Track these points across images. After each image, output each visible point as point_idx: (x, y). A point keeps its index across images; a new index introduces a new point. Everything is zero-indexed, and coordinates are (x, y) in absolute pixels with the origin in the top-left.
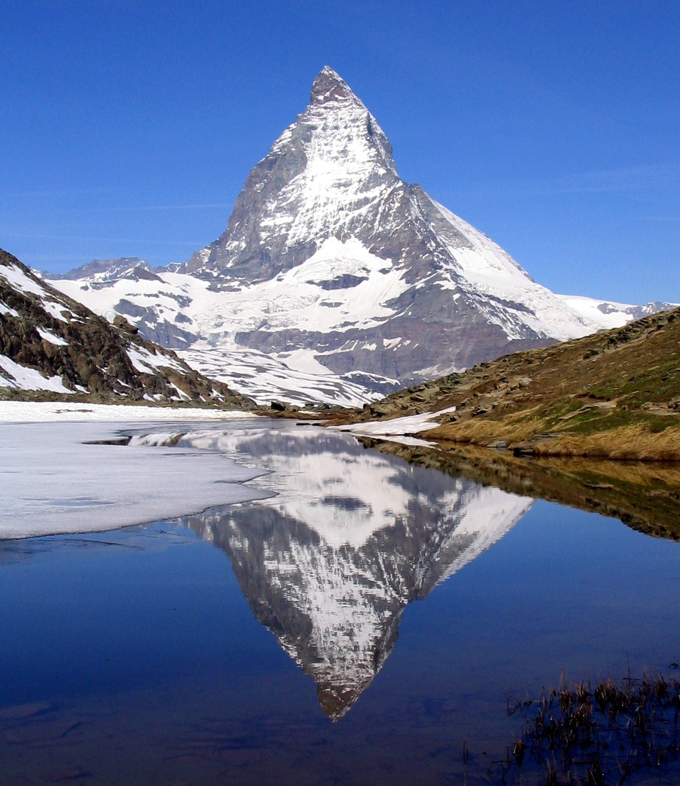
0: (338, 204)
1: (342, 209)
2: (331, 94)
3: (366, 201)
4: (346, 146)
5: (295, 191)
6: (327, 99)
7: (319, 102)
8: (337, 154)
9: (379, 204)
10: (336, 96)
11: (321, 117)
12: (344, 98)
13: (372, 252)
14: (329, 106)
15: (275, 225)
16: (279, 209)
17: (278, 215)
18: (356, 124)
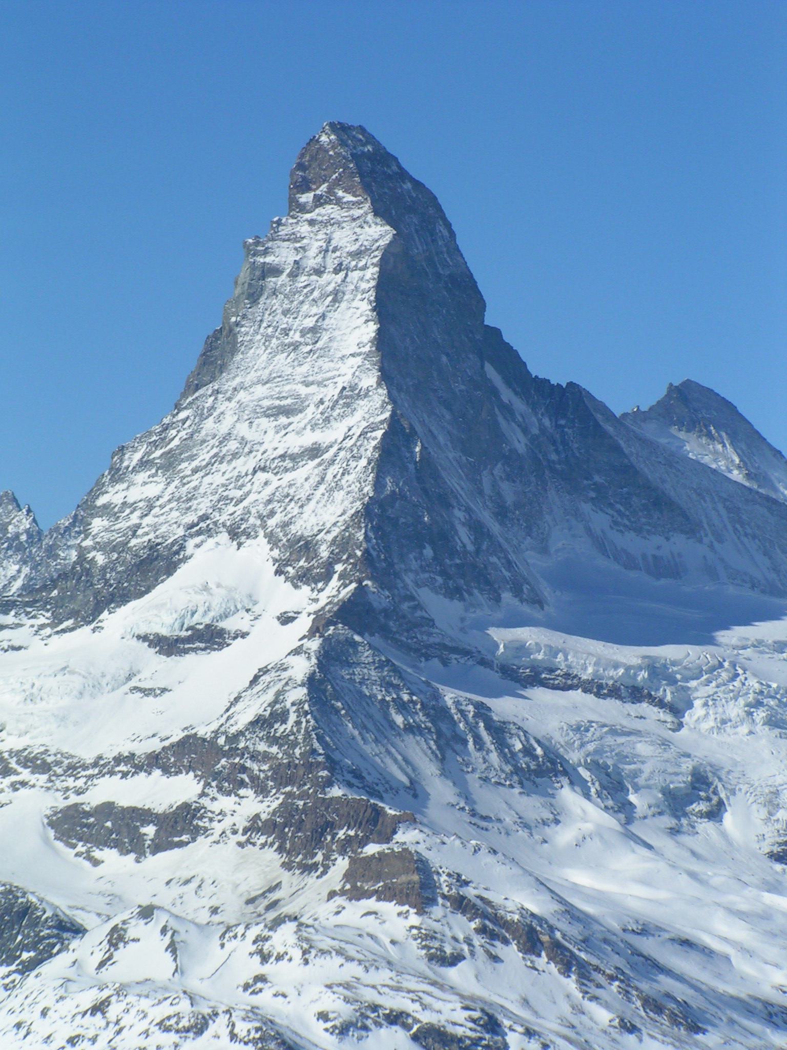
0: (259, 457)
1: (264, 469)
2: (330, 191)
4: (323, 317)
5: (188, 423)
6: (319, 201)
7: (303, 209)
8: (297, 337)
9: (332, 462)
10: (340, 193)
11: (298, 245)
12: (354, 199)
13: (278, 572)
14: (320, 218)
15: (124, 503)
16: (144, 464)
17: (142, 476)
18: (361, 264)
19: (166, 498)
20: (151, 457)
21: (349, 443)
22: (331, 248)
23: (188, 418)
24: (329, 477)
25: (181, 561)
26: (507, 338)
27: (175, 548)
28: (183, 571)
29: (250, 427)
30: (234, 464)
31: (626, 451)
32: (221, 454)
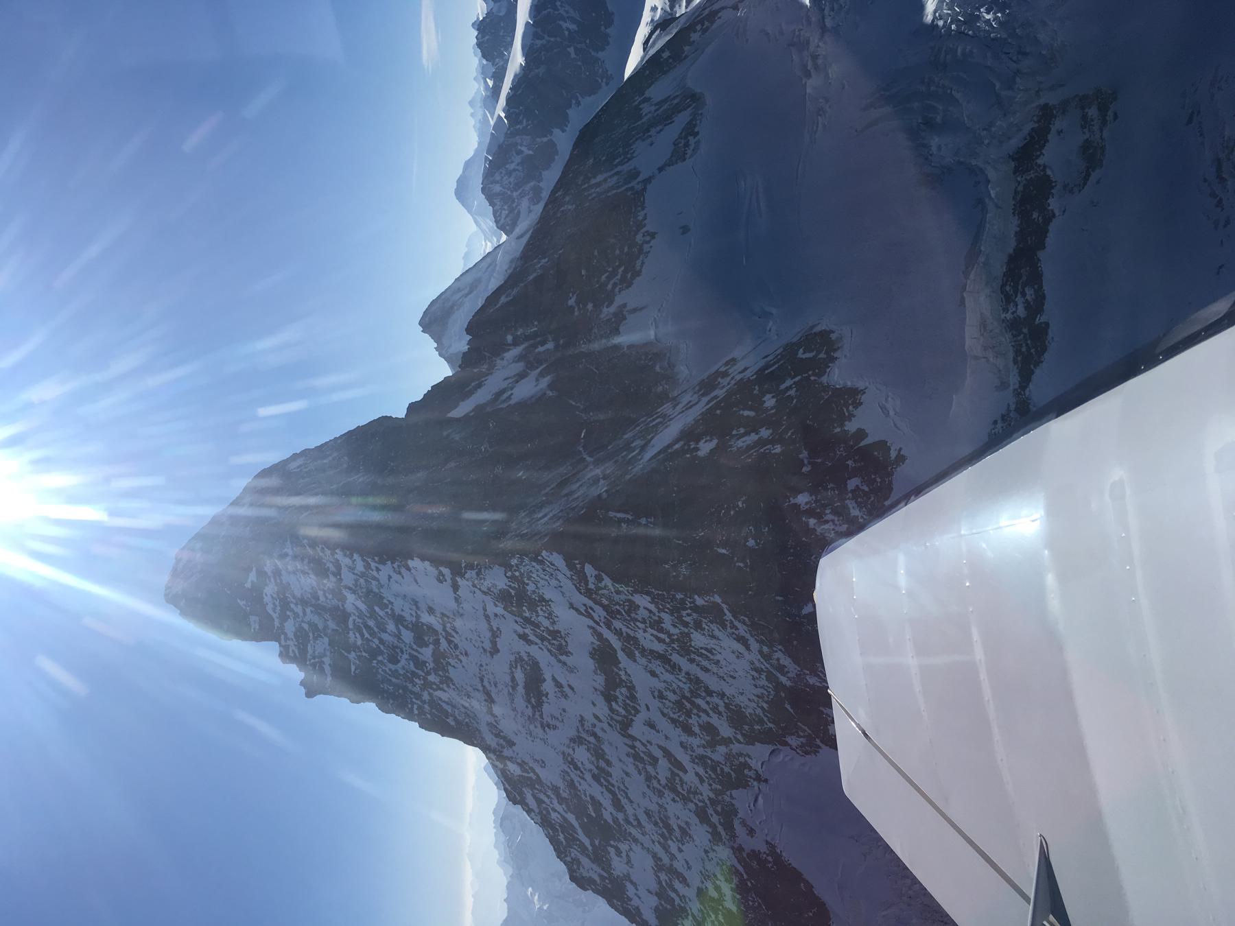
0: (606, 726)
3: (604, 657)
5: (542, 796)
19: (658, 849)
20: (590, 848)
21: (599, 613)
22: (314, 602)
23: (534, 796)
24: (659, 647)
25: (778, 858)
26: (419, 397)
27: (755, 864)
28: (793, 858)
29: (555, 728)
30: (613, 760)
31: (540, 272)
32: (596, 771)
